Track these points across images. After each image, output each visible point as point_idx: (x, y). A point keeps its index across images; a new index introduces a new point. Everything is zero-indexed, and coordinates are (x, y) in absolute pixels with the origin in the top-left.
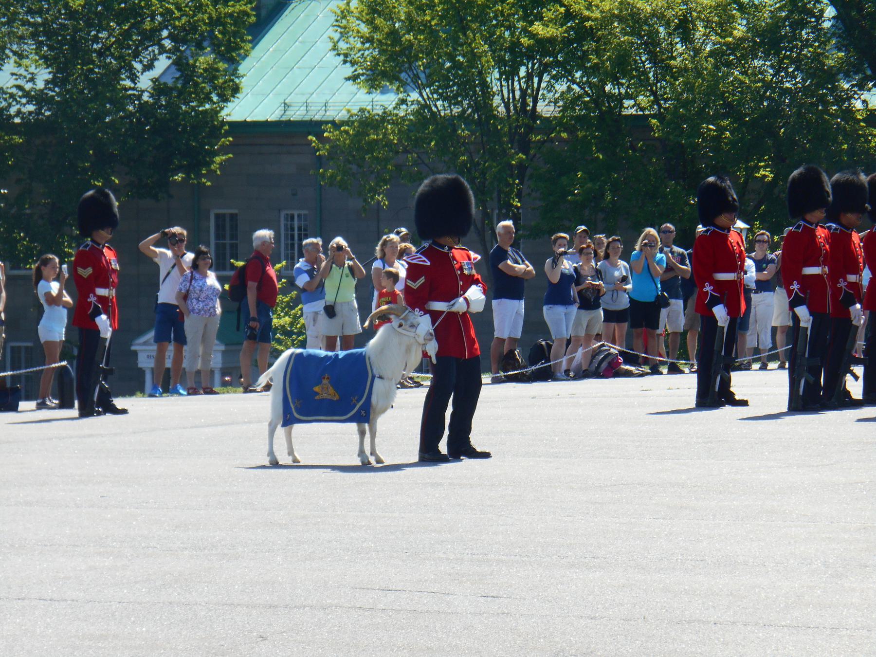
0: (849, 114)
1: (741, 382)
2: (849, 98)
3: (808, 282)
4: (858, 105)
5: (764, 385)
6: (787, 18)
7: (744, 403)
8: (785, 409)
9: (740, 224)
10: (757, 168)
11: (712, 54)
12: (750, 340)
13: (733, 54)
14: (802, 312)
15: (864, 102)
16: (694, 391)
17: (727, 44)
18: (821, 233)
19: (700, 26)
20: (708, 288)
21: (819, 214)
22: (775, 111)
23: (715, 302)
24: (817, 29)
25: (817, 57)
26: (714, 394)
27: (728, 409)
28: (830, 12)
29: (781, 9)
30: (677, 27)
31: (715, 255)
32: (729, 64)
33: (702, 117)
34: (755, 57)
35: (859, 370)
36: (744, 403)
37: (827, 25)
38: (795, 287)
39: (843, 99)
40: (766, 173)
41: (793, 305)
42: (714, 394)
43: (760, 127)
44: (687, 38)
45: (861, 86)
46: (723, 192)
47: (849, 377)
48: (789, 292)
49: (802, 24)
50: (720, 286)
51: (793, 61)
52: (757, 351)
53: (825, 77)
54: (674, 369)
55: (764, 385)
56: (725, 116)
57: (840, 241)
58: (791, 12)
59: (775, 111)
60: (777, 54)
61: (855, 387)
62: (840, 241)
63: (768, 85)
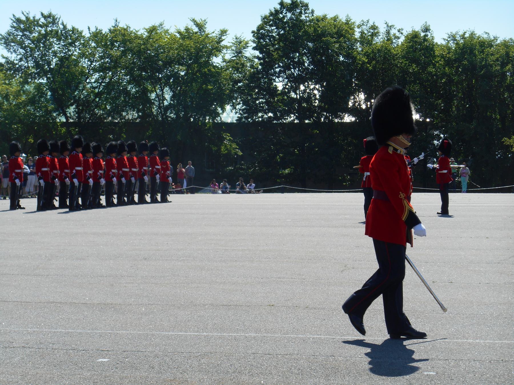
0: (55, 123)
1: (23, 202)
2: (55, 119)
3: (43, 173)
4: (58, 120)
5: (30, 203)
6: (37, 95)
7: (24, 208)
8: (36, 210)
9: (24, 155)
10: (29, 139)
11: (15, 105)
12: (27, 189)
13: (21, 105)
14: (42, 181)
15: (60, 120)
16: (9, 205)
17: (20, 102)
18: (48, 159)
19: (12, 97)
20: (14, 174)
21: (47, 152)
22: (33, 122)
23: (16, 178)
24: (46, 99)
25: (46, 106)
26: (15, 206)
27: (19, 210)
28: (49, 93)
29: (36, 92)
30: (4, 97)
31: (15, 165)
32: (20, 108)
33: (12, 123)
34: (28, 106)
35: (57, 198)
36: (24, 208)
37: (48, 97)
38: (39, 174)
39: (54, 119)
40: (31, 140)
41: (39, 179)
42: (15, 206)
43: (30, 126)
44: (8, 100)
45: (59, 115)
46: (16, 146)
47: (54, 201)
48: (38, 176)
49: (41, 97)
50: (17, 174)
51: (39, 107)
52: (29, 192)
53: (48, 113)
54: (5, 198)
55: (30, 203)
56: (19, 123)
57: (52, 160)
58: (38, 93)
59: (33, 122)
60: (34, 105)
61: (56, 204)
62: (52, 160)
63: (32, 114)
